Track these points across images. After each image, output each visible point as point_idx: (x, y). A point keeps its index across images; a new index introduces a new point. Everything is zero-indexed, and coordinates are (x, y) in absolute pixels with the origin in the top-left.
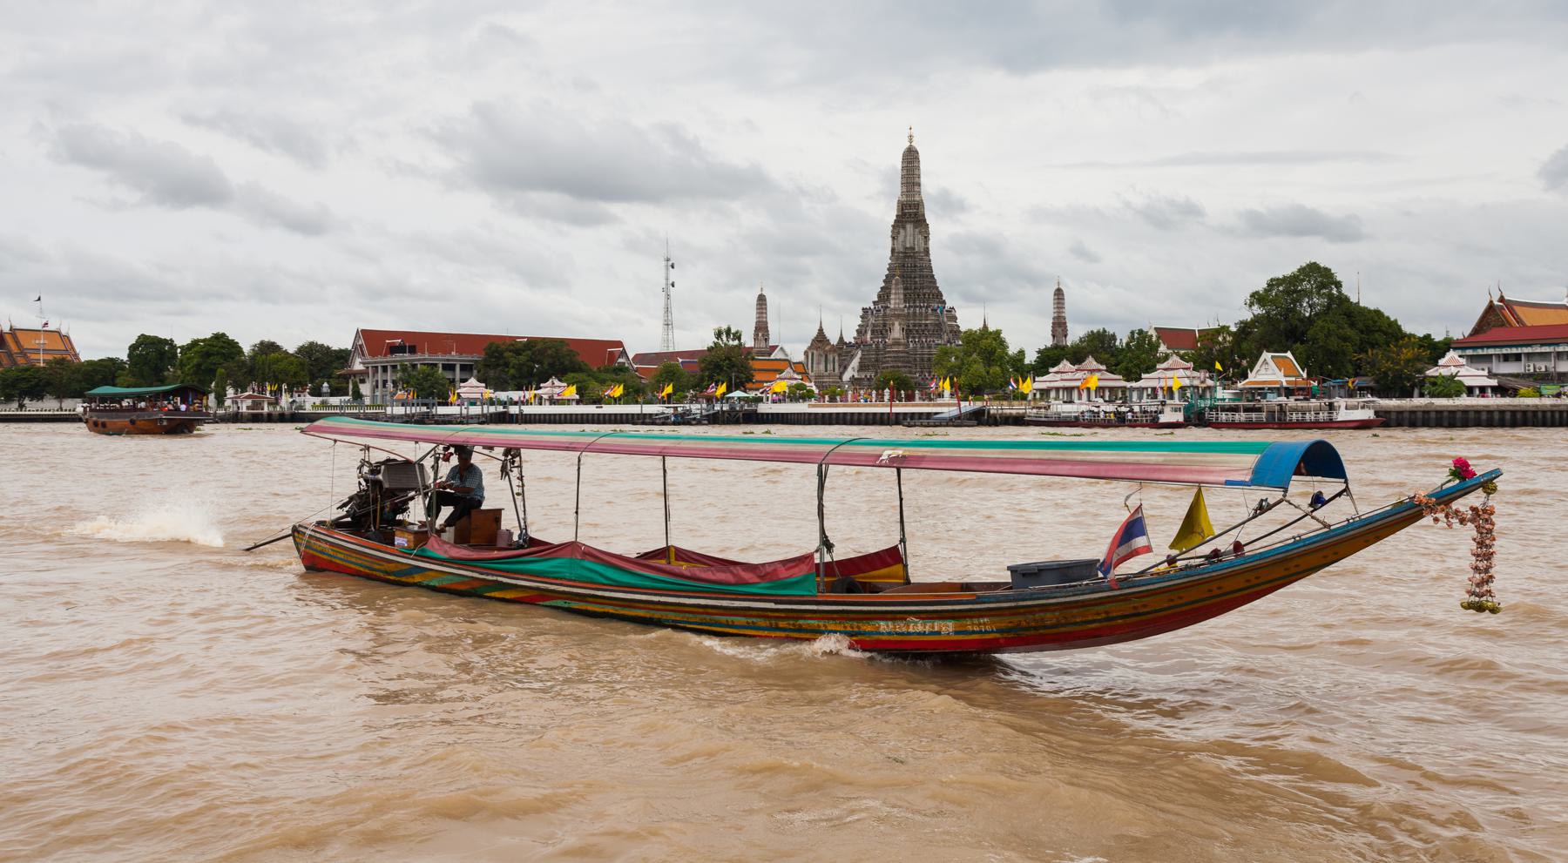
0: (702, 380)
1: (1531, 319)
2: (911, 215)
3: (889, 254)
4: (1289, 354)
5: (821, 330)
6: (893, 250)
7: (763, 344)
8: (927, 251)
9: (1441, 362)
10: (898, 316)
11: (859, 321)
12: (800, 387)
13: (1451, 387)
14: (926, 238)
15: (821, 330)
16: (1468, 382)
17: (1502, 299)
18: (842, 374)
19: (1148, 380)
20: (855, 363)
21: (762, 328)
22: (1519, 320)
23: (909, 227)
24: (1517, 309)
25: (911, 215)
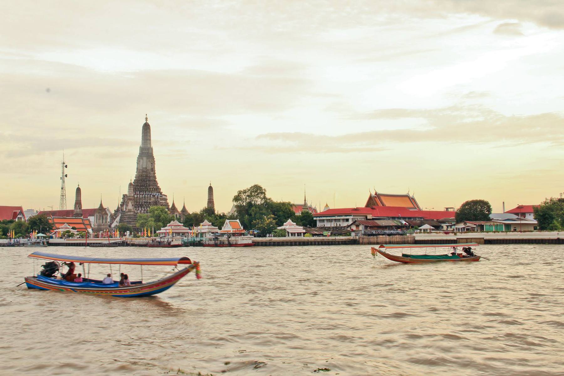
0: (28, 228)
1: (388, 203)
2: (146, 153)
3: (136, 170)
4: (238, 221)
5: (101, 205)
6: (137, 169)
7: (78, 210)
8: (153, 170)
9: (284, 224)
10: (131, 199)
11: (122, 200)
12: (69, 232)
13: (284, 233)
14: (153, 163)
15: (101, 205)
16: (290, 231)
17: (376, 194)
18: (111, 224)
19: (196, 230)
20: (118, 219)
21: (78, 203)
22: (382, 202)
23: (145, 158)
24: (382, 198)
25: (146, 153)
